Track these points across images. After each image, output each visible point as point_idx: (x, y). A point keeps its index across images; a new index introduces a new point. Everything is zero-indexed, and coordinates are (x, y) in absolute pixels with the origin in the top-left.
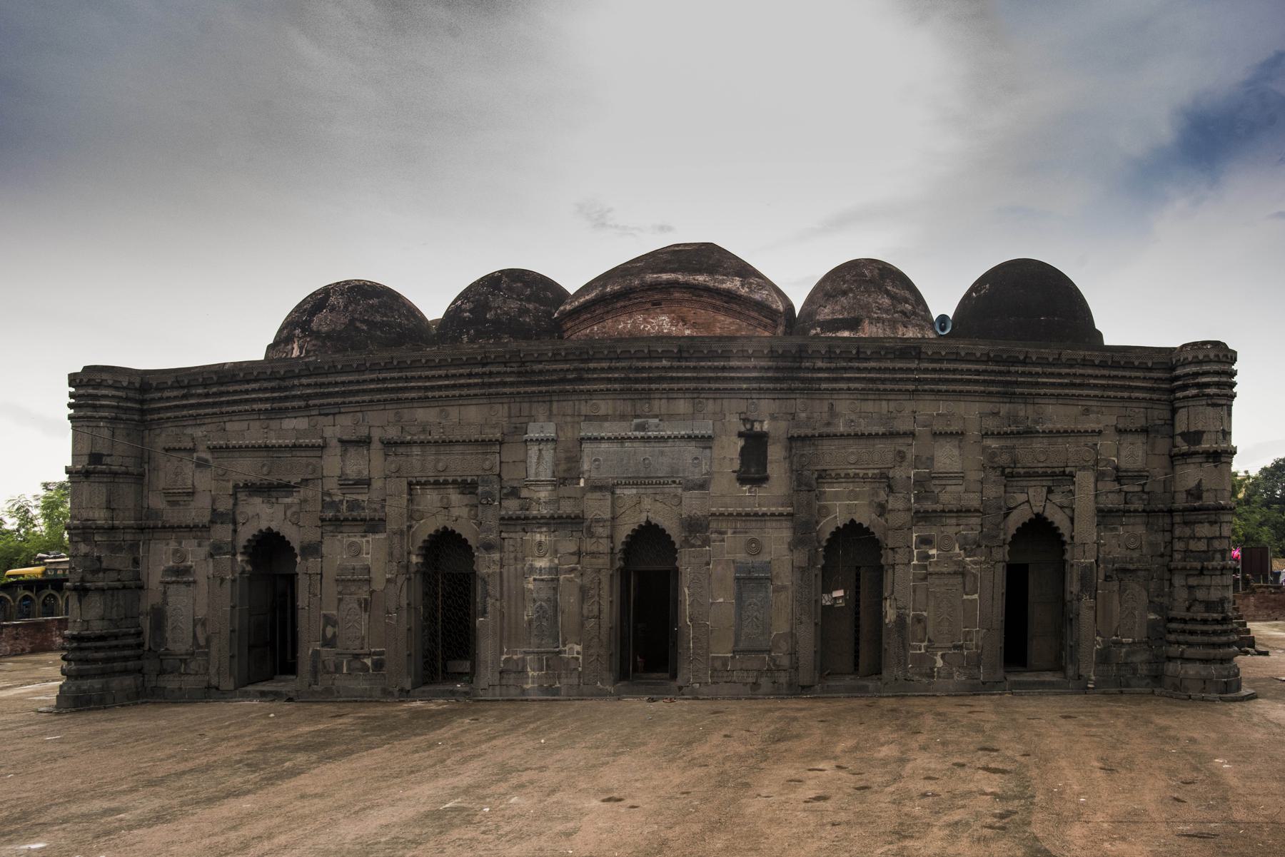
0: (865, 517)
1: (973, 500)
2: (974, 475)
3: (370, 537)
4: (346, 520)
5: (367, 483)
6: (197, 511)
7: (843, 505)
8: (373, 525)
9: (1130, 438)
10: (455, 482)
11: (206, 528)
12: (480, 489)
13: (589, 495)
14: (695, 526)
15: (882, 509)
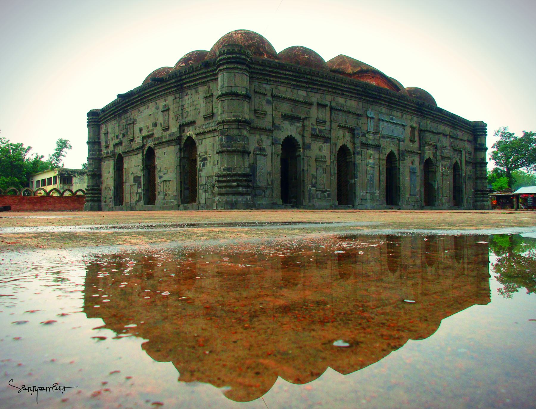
0: (431, 157)
1: (448, 155)
2: (449, 148)
3: (325, 144)
4: (320, 136)
5: (325, 122)
6: (266, 123)
7: (428, 154)
8: (327, 140)
9: (469, 143)
10: (347, 128)
11: (273, 131)
12: (356, 132)
13: (381, 139)
14: (403, 154)
15: (435, 155)
